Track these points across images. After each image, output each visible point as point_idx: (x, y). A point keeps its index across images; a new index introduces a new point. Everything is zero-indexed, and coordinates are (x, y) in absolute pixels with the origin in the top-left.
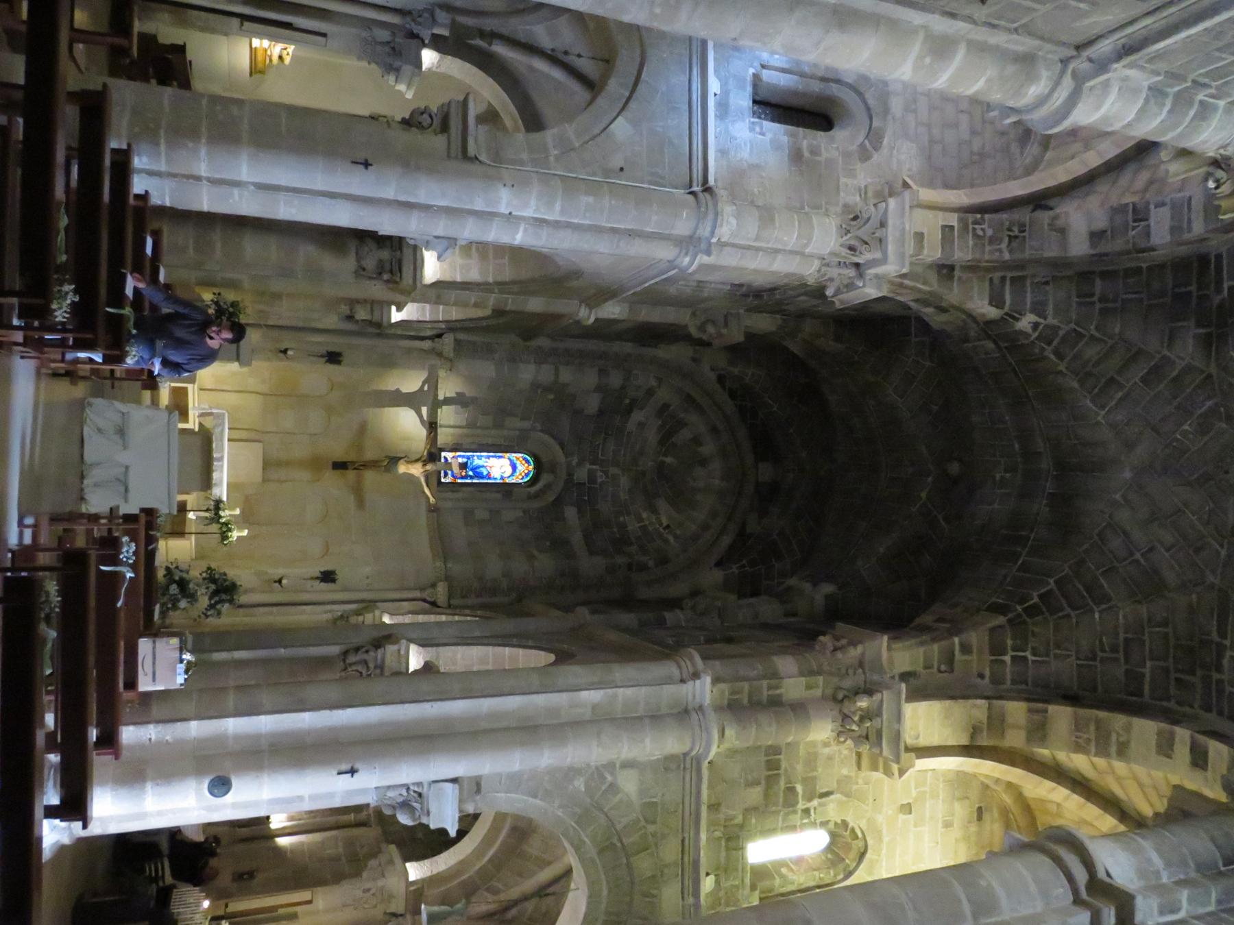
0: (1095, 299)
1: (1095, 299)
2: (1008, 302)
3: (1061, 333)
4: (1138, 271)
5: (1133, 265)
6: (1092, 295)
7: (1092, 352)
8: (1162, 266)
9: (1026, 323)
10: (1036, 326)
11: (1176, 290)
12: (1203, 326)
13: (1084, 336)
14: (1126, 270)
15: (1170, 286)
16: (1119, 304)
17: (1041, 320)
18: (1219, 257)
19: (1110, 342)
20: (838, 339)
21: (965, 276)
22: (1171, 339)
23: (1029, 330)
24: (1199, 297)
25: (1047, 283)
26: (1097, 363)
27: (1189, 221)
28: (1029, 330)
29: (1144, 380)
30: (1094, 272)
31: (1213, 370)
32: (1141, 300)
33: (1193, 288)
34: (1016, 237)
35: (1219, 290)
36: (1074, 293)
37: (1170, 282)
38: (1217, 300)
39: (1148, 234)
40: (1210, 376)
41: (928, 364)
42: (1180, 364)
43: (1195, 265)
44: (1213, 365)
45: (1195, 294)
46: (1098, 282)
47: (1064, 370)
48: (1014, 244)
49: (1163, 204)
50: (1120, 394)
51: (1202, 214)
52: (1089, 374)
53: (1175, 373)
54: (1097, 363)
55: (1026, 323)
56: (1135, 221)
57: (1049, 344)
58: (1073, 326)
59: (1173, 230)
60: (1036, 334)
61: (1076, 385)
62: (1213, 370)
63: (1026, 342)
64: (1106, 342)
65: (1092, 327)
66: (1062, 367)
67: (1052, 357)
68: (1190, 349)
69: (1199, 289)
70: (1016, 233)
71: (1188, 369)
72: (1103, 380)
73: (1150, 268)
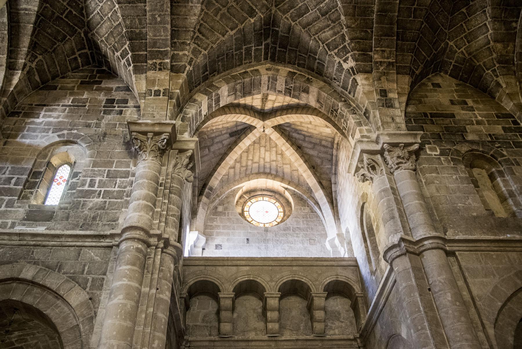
0: (318, 61)
1: (318, 61)
2: (351, 80)
3: (336, 51)
4: (299, 65)
5: (300, 68)
6: (318, 63)
7: (327, 34)
8: (289, 63)
9: (351, 63)
10: (345, 61)
11: (285, 50)
12: (275, 30)
13: (326, 45)
14: (304, 68)
15: (287, 53)
16: (309, 53)
17: (342, 62)
18: (266, 59)
19: (316, 36)
20: (498, 85)
21: (361, 106)
22: (289, 29)
23: (350, 58)
24: (276, 44)
25: (335, 79)
26: (328, 26)
27: (269, 82)
28: (350, 58)
29: (307, 10)
30: (316, 73)
31: (274, 9)
32: (300, 52)
33: (278, 49)
34: (335, 110)
35: (267, 46)
36: (325, 68)
37: (287, 55)
38: (269, 41)
39: (286, 82)
40: (276, 6)
41: (451, 43)
42: (288, 15)
43: (276, 58)
44: (273, 12)
45: (278, 46)
46: (315, 68)
47: (345, 27)
48: (336, 108)
49: (279, 91)
50: (321, 6)
51: (262, 83)
52: (333, 22)
53: (291, 11)
54: (328, 26)
55: (351, 63)
56: (291, 90)
57: (345, 46)
58: (329, 53)
59: (276, 81)
60: (348, 55)
61: (343, 17)
62: (274, 9)
63: (356, 52)
64: (318, 37)
65: (321, 48)
66: (345, 30)
67: (347, 38)
68: (282, 21)
69: (276, 48)
70: (334, 112)
71: (285, 12)
72: (327, 16)
73: (294, 64)
